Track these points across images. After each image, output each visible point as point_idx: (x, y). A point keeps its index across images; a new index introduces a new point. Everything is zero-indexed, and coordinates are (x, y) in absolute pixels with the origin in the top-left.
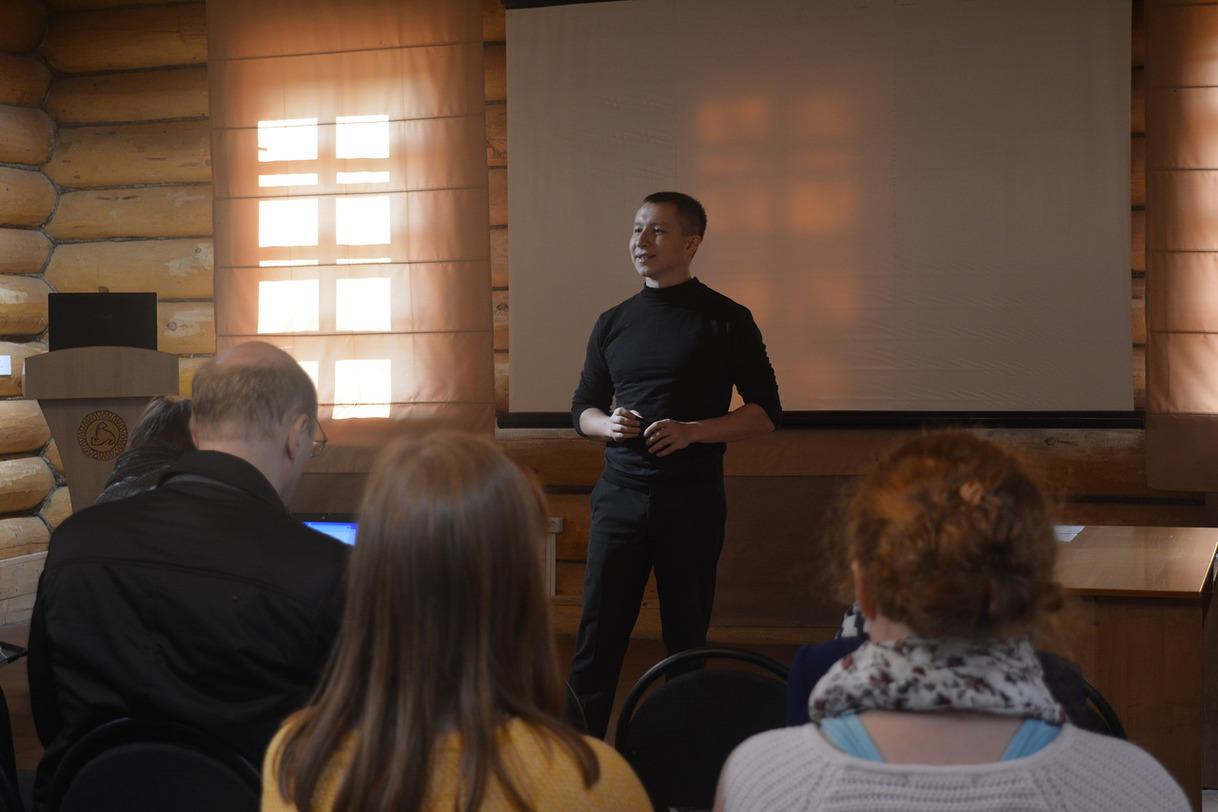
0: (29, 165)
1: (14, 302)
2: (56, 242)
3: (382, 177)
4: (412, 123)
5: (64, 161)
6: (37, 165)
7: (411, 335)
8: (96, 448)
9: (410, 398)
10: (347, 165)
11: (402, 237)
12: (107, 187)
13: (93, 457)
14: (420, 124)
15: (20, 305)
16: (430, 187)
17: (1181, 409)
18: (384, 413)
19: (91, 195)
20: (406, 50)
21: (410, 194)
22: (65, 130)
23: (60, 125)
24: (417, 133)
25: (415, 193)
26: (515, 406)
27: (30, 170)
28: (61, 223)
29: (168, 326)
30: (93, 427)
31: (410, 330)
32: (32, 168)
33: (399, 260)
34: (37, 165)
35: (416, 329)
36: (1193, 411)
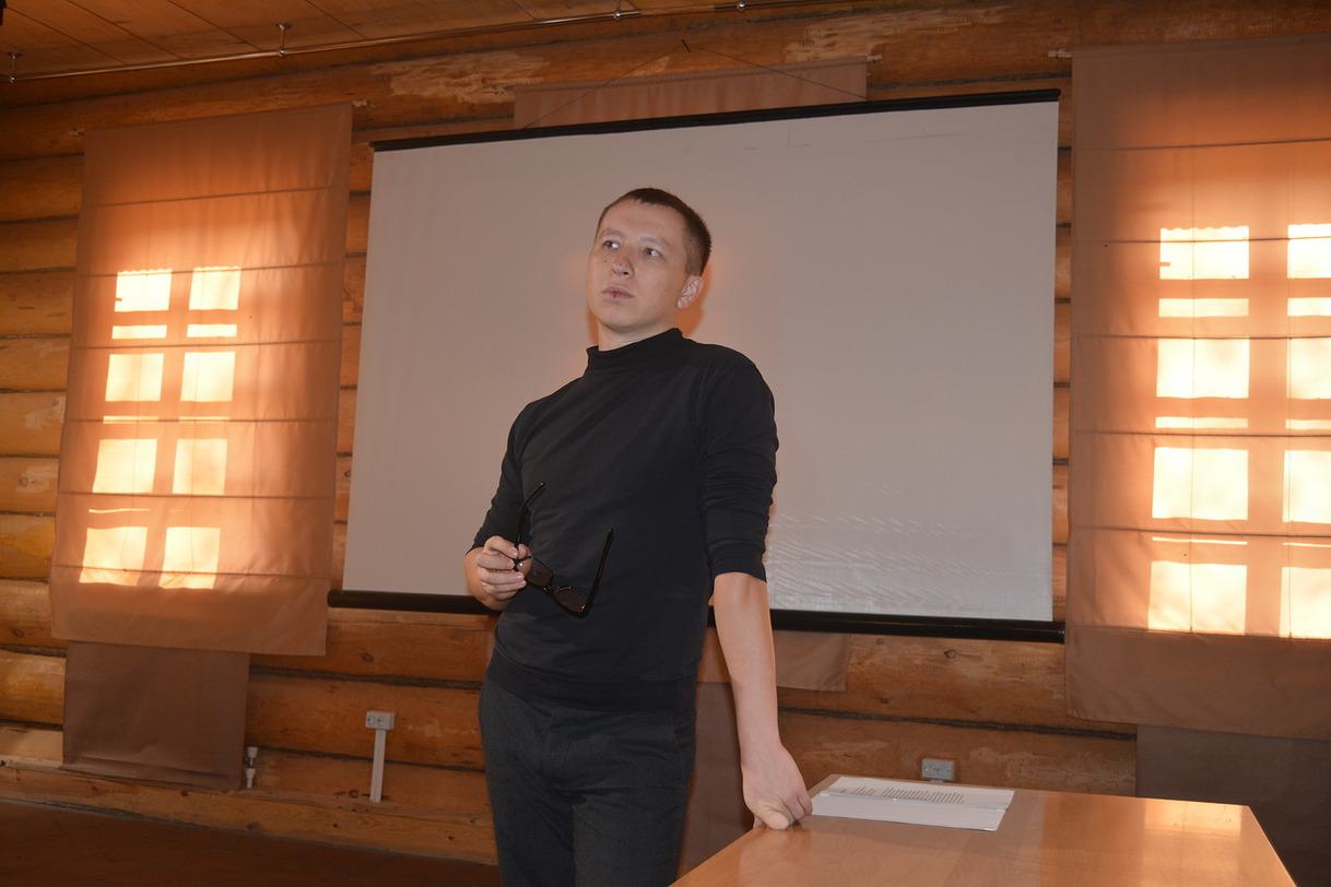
3: (228, 331)
4: (271, 271)
7: (250, 500)
9: (244, 569)
10: (203, 317)
11: (245, 393)
14: (279, 273)
16: (283, 340)
17: (1109, 621)
18: (207, 583)
20: (272, 196)
21: (263, 347)
24: (275, 282)
25: (268, 347)
26: (351, 584)
29: (20, 481)
31: (250, 494)
33: (245, 417)
35: (257, 493)
36: (1123, 624)
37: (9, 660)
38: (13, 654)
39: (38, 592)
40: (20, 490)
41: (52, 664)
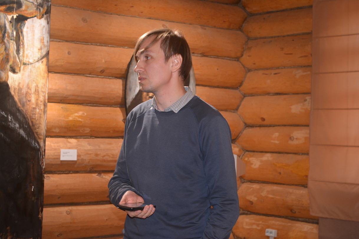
0: (233, 58)
2: (245, 96)
5: (249, 56)
12: (267, 69)
19: (261, 72)
23: (249, 39)
27: (233, 60)
28: (247, 86)
29: (290, 138)
32: (234, 59)
37: (289, 224)
38: (290, 221)
39: (302, 192)
40: (290, 142)
41: (311, 227)
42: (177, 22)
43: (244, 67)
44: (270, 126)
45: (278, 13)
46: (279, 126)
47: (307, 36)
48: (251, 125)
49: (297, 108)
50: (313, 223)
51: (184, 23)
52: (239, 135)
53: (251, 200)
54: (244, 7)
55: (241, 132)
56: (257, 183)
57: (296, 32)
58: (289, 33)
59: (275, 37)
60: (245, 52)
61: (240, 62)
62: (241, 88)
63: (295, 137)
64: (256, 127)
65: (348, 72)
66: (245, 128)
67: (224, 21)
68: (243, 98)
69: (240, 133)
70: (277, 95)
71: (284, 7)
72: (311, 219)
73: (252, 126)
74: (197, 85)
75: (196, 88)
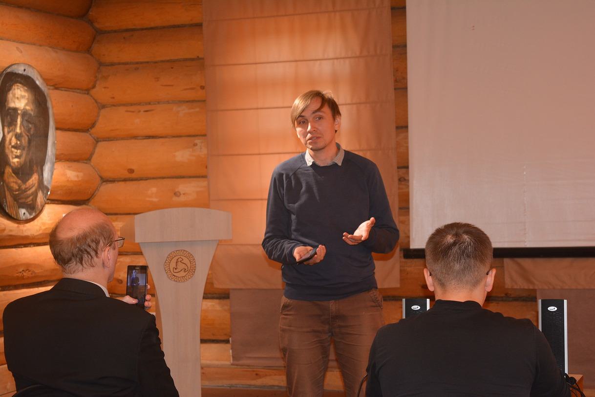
1: (76, 179)
2: (97, 140)
4: (342, 61)
5: (105, 88)
6: (86, 90)
8: (175, 274)
13: (174, 281)
15: (79, 181)
19: (122, 110)
22: (102, 67)
25: (344, 106)
27: (83, 94)
30: (174, 260)
32: (84, 92)
34: (86, 90)
42: (28, 44)
43: (96, 102)
44: (141, 179)
45: (144, 31)
46: (153, 178)
47: (198, 63)
48: (111, 179)
49: (182, 155)
50: (213, 298)
51: (34, 44)
52: (95, 194)
53: (120, 278)
54: (91, 22)
55: (97, 188)
56: (126, 255)
57: (173, 58)
58: (163, 58)
59: (141, 63)
60: (98, 82)
61: (91, 96)
62: (93, 131)
63: (181, 193)
64: (120, 181)
65: (257, 109)
66: (102, 183)
67: (74, 42)
68: (96, 144)
69: (96, 191)
70: (150, 138)
71: (153, 25)
72: (210, 294)
73: (113, 181)
74: (57, 129)
75: (56, 132)
